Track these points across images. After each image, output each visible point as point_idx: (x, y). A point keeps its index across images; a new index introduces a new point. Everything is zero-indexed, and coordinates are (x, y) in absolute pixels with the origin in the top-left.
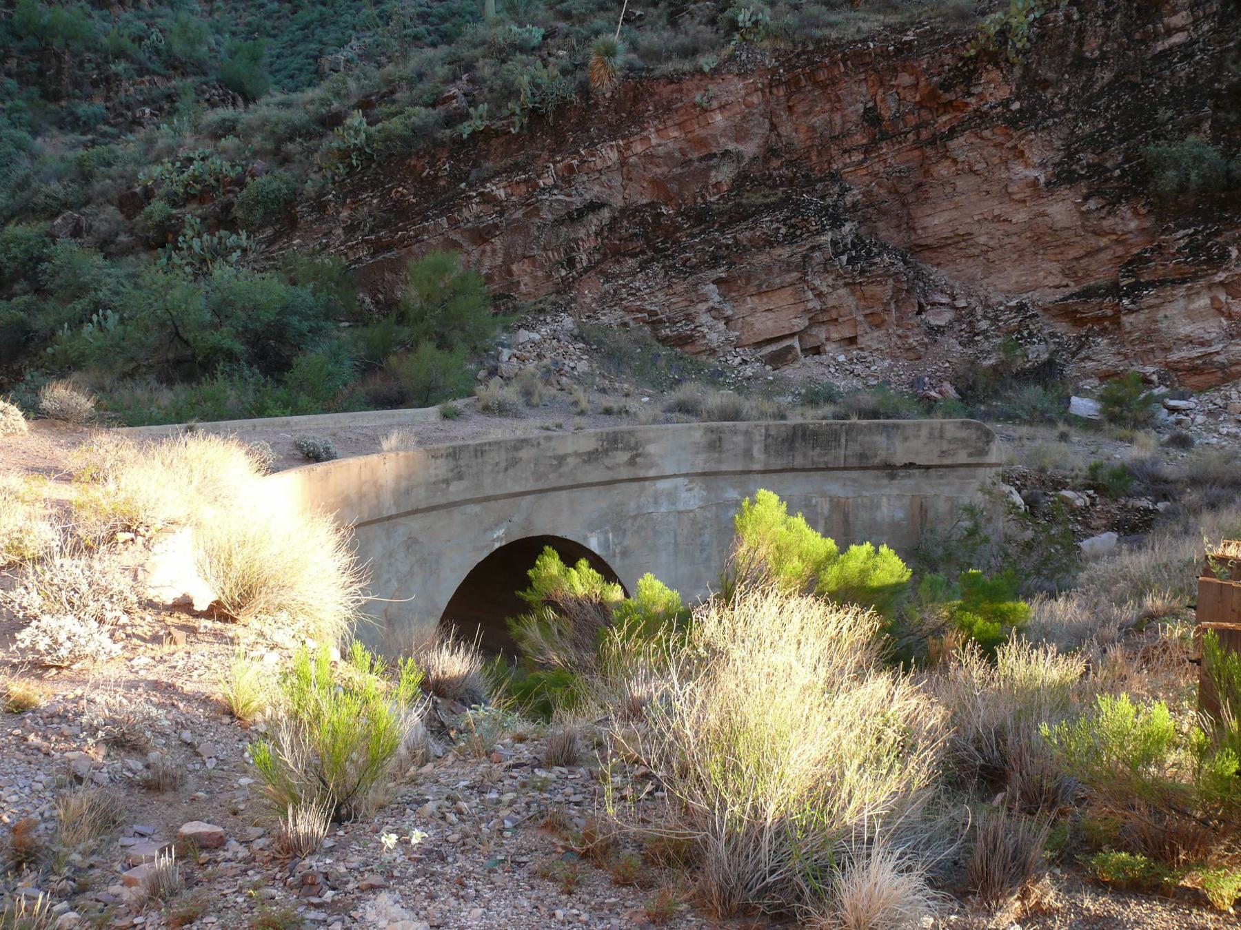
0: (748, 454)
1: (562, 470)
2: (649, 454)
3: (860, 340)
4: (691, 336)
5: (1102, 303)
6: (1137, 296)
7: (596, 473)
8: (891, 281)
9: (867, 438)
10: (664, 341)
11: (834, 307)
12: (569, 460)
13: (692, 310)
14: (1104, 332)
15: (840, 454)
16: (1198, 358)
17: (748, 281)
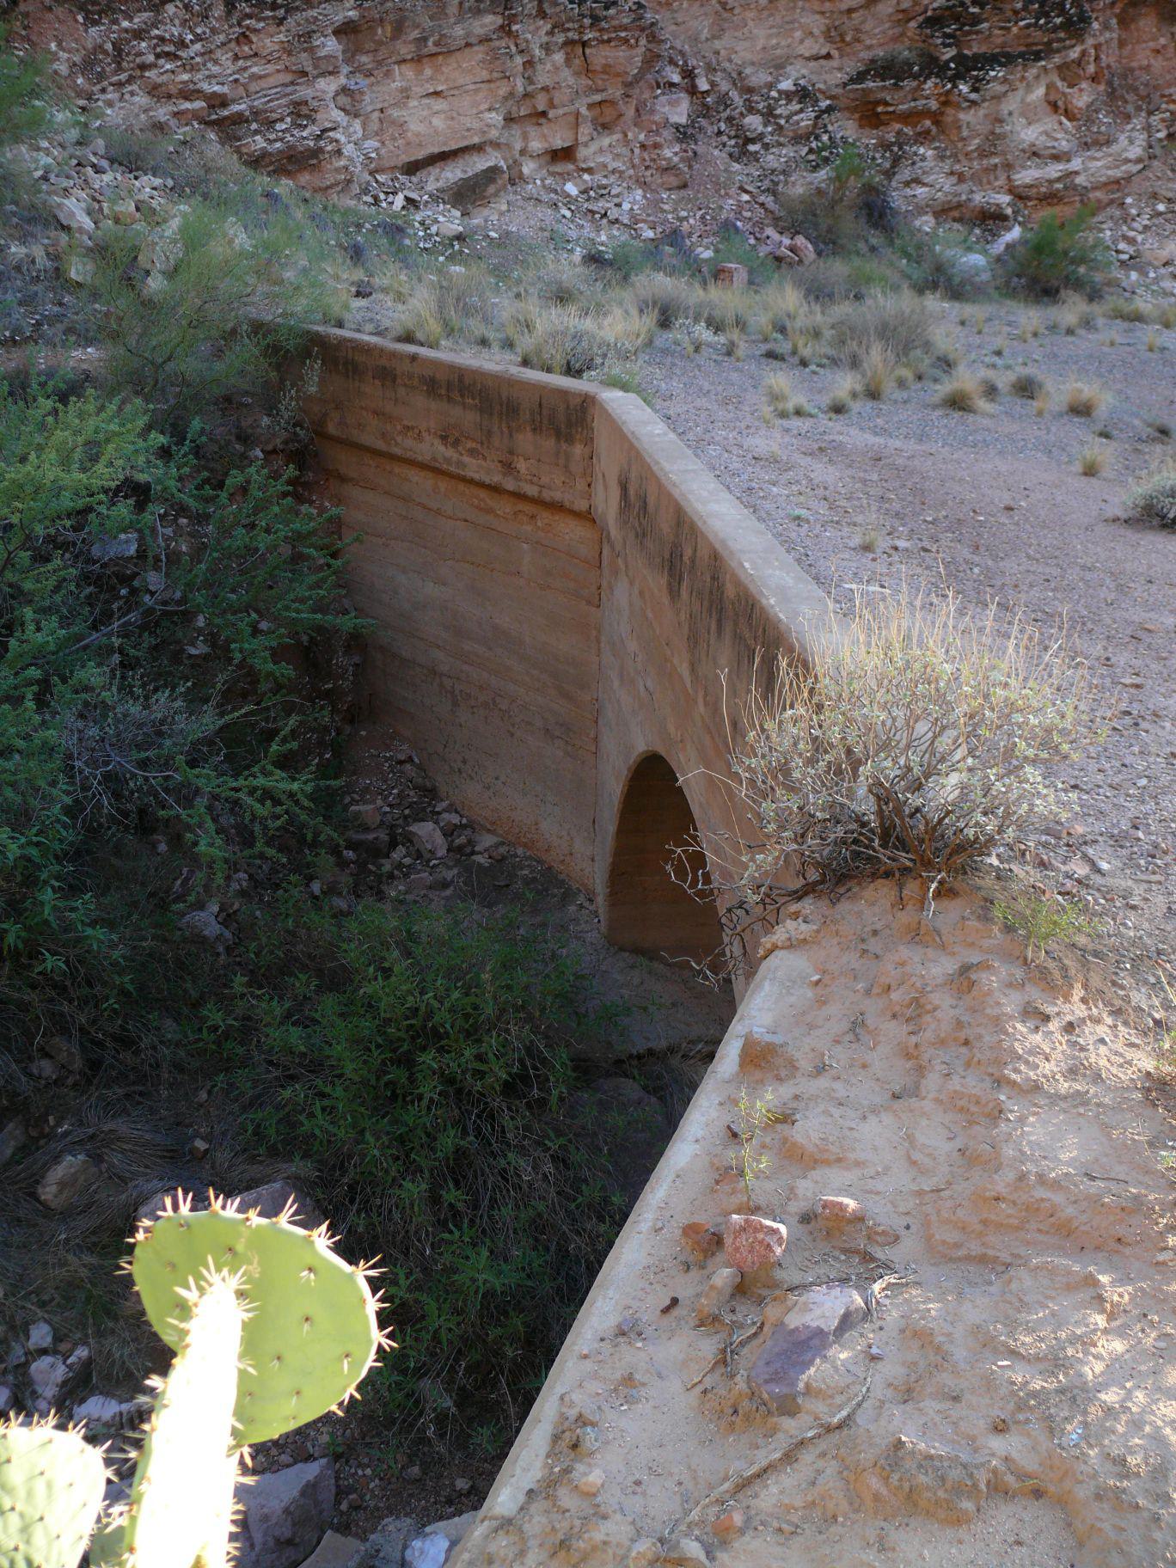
3: (582, 152)
4: (316, 152)
5: (919, 88)
6: (978, 80)
8: (643, 42)
10: (256, 162)
11: (545, 89)
13: (304, 92)
14: (924, 137)
16: (1059, 180)
17: (398, 29)
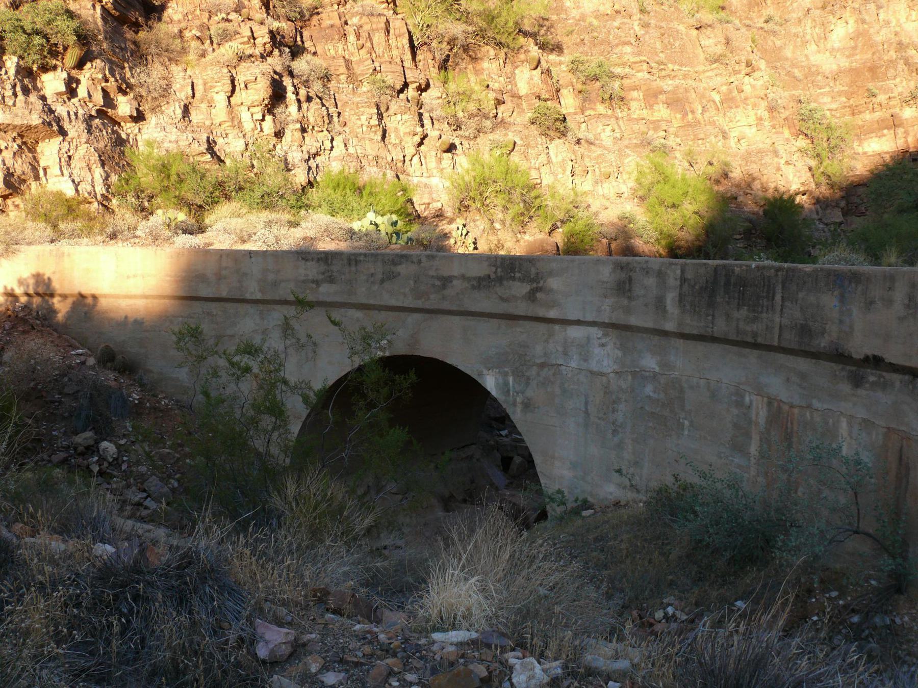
0: (660, 304)
1: (446, 292)
2: (551, 291)
7: (483, 302)
9: (812, 299)
12: (455, 282)
15: (776, 321)
